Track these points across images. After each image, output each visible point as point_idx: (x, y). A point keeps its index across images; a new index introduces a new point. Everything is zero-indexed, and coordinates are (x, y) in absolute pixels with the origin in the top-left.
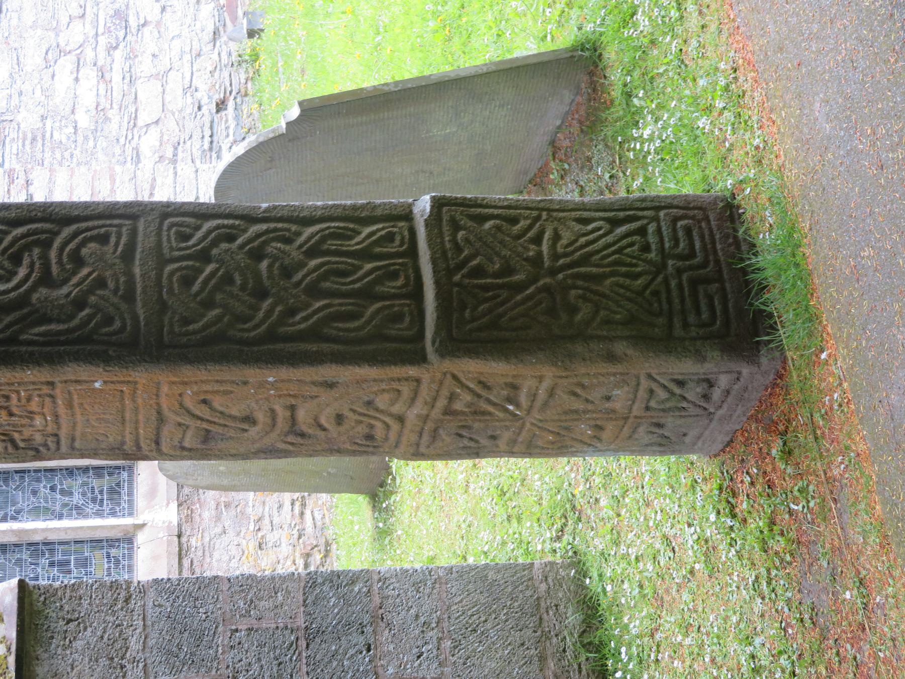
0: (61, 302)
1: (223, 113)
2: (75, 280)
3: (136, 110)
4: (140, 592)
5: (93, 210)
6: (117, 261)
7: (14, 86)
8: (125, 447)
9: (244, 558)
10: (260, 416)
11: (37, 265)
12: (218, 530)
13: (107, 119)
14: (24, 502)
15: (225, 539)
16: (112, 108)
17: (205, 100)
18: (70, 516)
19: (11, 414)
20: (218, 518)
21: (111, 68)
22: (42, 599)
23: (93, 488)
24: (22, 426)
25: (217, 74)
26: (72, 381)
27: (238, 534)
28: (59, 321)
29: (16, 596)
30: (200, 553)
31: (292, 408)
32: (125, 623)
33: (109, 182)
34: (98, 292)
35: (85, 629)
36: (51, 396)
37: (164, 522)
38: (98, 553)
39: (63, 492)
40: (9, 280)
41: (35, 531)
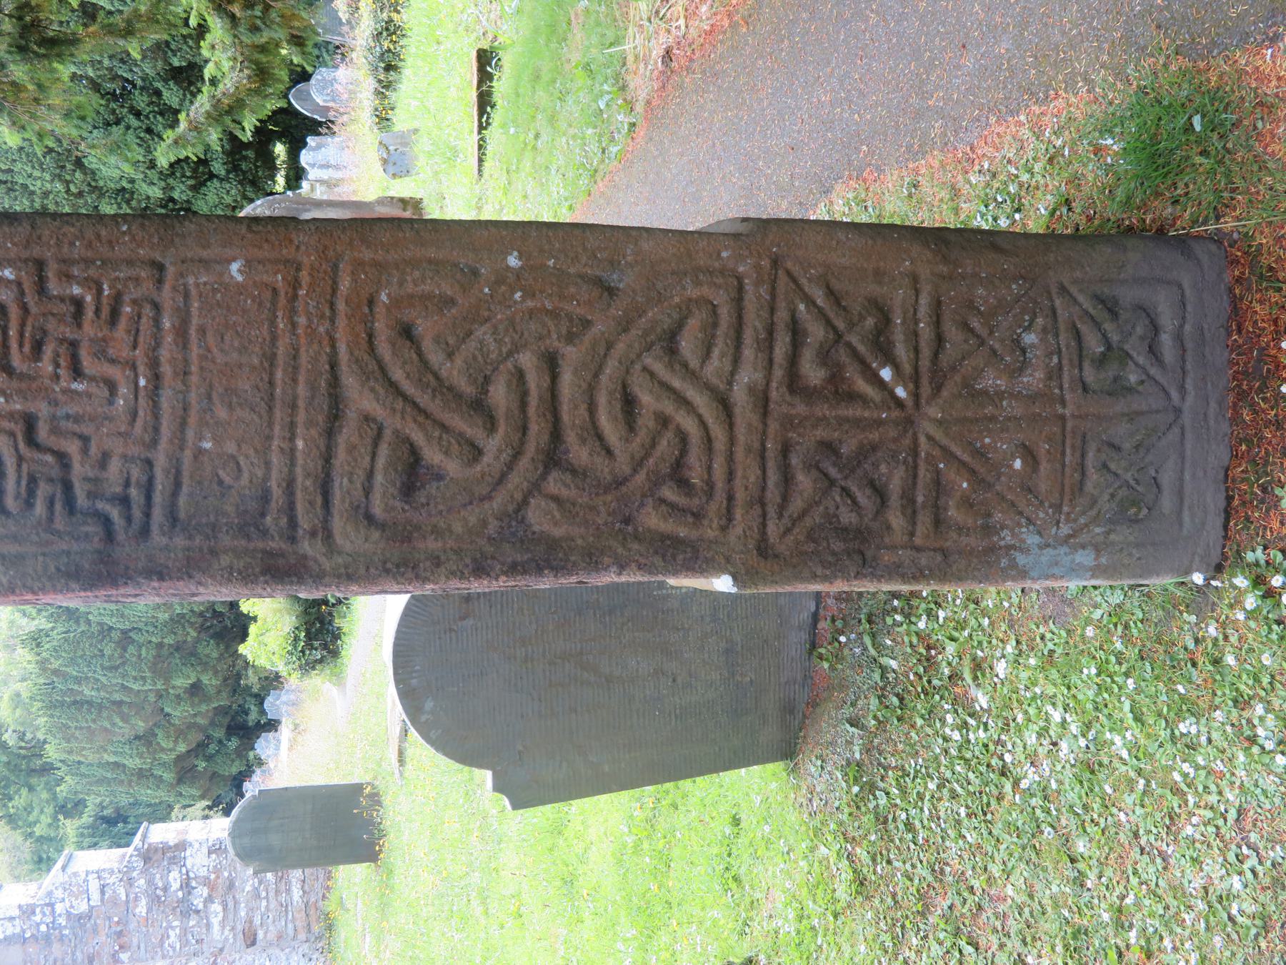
10: (499, 394)
19: (77, 373)
31: (551, 363)
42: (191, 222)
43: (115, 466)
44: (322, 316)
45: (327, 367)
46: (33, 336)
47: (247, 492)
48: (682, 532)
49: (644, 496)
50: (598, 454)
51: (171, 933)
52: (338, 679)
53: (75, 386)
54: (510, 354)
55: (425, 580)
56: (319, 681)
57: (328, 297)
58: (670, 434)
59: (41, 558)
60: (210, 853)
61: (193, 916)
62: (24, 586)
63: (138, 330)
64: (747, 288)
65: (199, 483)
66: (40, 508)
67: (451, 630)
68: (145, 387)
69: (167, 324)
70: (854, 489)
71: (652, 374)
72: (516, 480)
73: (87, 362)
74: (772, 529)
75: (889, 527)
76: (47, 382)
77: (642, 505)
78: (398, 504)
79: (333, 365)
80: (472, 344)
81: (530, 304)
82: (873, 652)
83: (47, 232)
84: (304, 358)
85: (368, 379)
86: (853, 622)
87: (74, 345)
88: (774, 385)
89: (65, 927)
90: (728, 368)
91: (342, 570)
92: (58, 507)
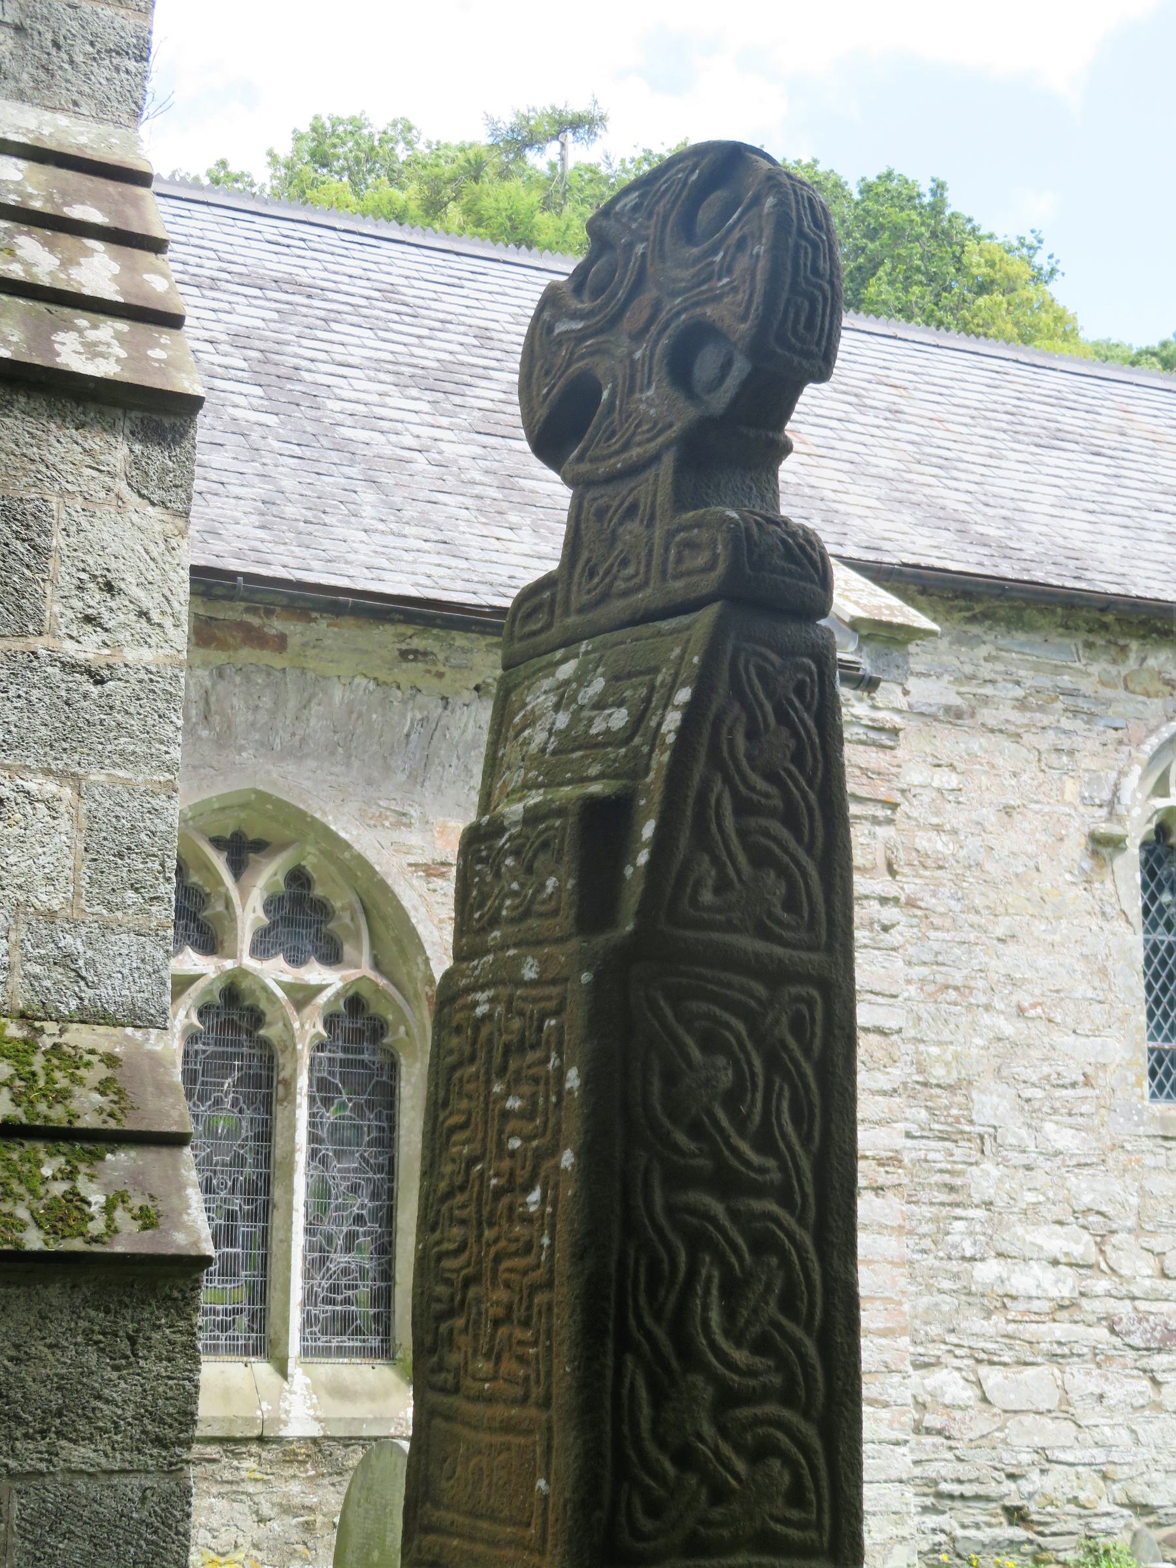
0: (688, 1426)
1: (1003, 1519)
2: (726, 1449)
3: (1005, 1364)
4: (171, 1464)
5: (847, 1478)
6: (758, 1523)
7: (1041, 1158)
8: (428, 1505)
9: (213, 1555)
11: (752, 1382)
12: (266, 1510)
13: (988, 1314)
14: (340, 1171)
15: (249, 1522)
16: (1009, 1321)
17: (1026, 1486)
18: (310, 1247)
19: (497, 1323)
20: (286, 1510)
21: (1076, 1322)
22: (176, 1294)
23: (357, 1287)
24: (476, 1337)
25: (1072, 1508)
26: (550, 1439)
27: (256, 1546)
28: (656, 1422)
29: (184, 1252)
30: (227, 1475)
32: (119, 1438)
33: (881, 1325)
34: (704, 1491)
35: (116, 1368)
36: (525, 1398)
37: (287, 1412)
38: (243, 1294)
39: (351, 1237)
40: (727, 1333)
41: (290, 1190)
42: (576, 1438)
87: (507, 1318)
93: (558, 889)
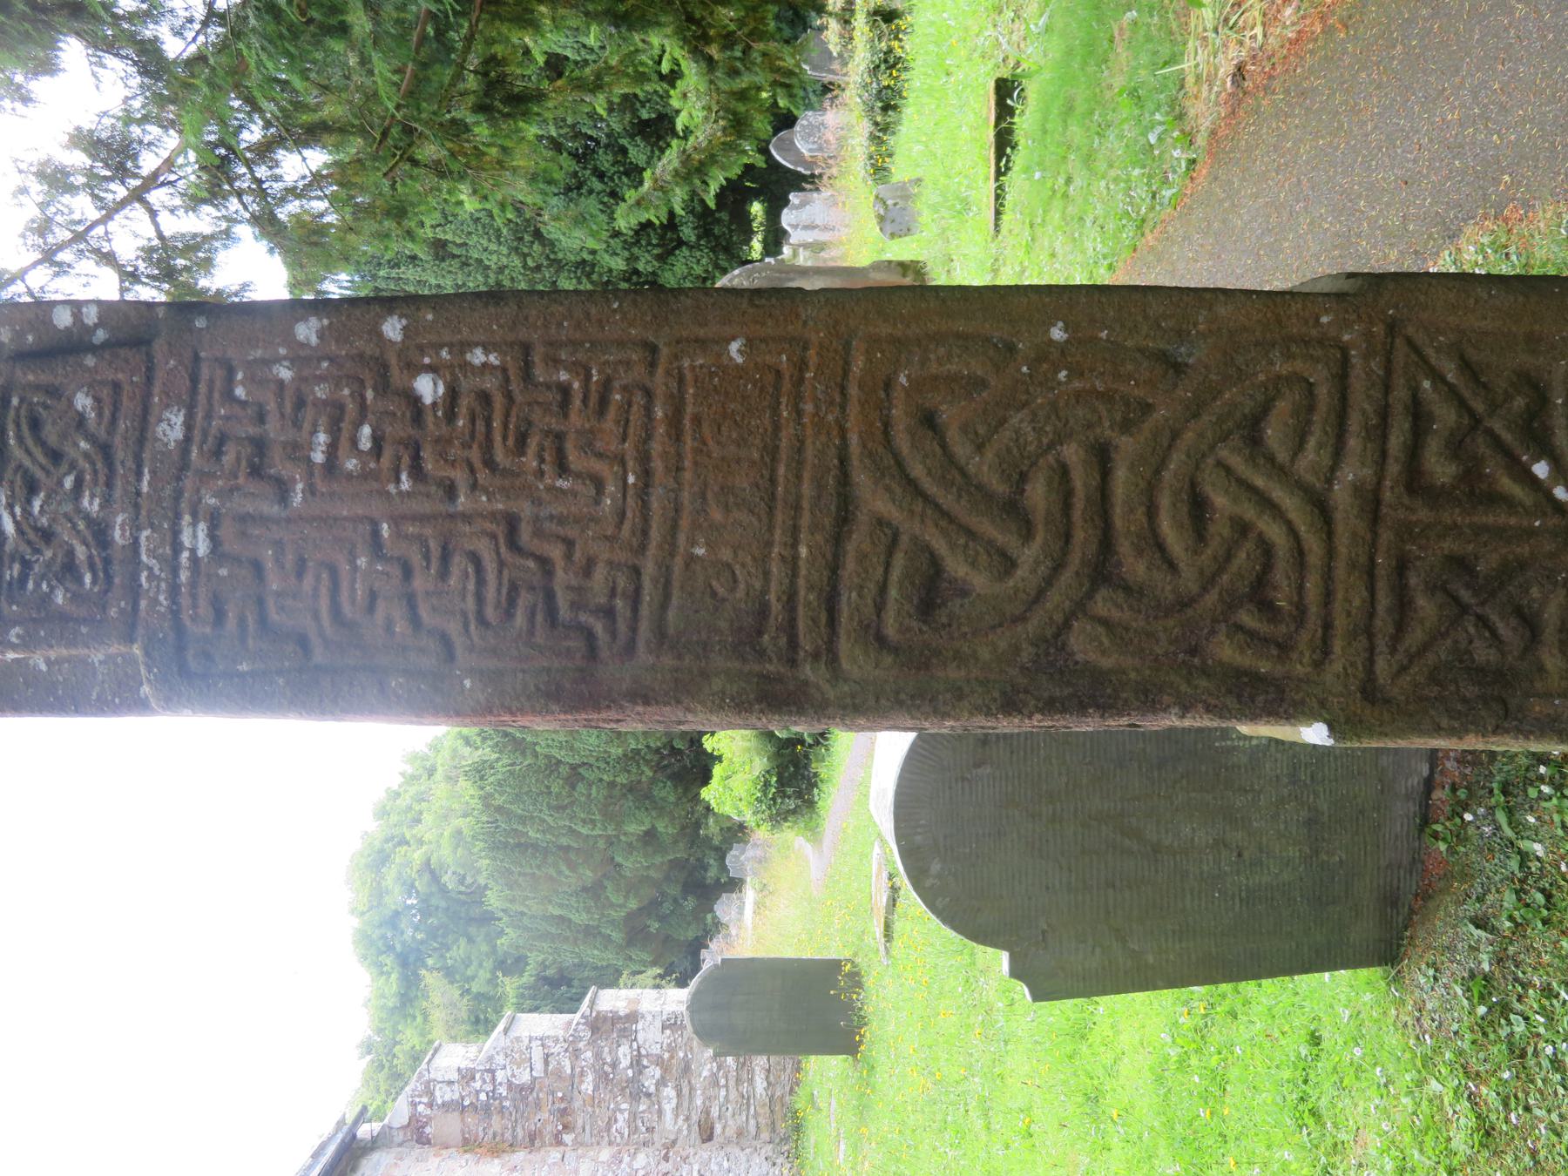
10: (1038, 494)
19: (563, 468)
31: (1102, 456)
43: (600, 573)
44: (832, 403)
45: (836, 461)
46: (517, 427)
47: (743, 606)
48: (1264, 668)
49: (1215, 621)
50: (1158, 568)
51: (619, 1116)
52: (814, 833)
53: (560, 483)
54: (1051, 445)
55: (945, 716)
56: (792, 837)
57: (839, 380)
58: (1249, 545)
59: (520, 676)
60: (664, 1028)
61: (644, 1099)
62: (502, 705)
63: (627, 421)
64: (1354, 361)
65: (691, 594)
66: (520, 620)
67: (963, 779)
68: (634, 484)
69: (659, 413)
70: (1494, 618)
71: (1228, 470)
72: (1057, 599)
73: (574, 458)
74: (1382, 666)
75: (1541, 669)
76: (530, 478)
77: (1213, 632)
78: (914, 624)
79: (843, 461)
80: (1006, 434)
81: (1077, 384)
82: (1509, 832)
83: (534, 312)
84: (809, 452)
85: (883, 475)
86: (1482, 792)
87: (560, 437)
88: (1388, 483)
89: (506, 1098)
90: (1327, 461)
91: (848, 700)
92: (539, 618)
93: (92, 387)
